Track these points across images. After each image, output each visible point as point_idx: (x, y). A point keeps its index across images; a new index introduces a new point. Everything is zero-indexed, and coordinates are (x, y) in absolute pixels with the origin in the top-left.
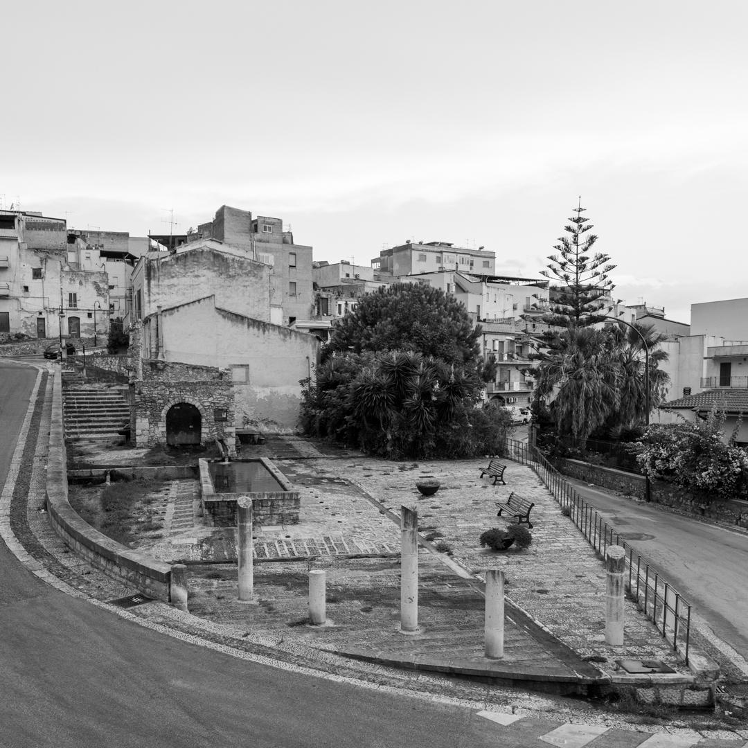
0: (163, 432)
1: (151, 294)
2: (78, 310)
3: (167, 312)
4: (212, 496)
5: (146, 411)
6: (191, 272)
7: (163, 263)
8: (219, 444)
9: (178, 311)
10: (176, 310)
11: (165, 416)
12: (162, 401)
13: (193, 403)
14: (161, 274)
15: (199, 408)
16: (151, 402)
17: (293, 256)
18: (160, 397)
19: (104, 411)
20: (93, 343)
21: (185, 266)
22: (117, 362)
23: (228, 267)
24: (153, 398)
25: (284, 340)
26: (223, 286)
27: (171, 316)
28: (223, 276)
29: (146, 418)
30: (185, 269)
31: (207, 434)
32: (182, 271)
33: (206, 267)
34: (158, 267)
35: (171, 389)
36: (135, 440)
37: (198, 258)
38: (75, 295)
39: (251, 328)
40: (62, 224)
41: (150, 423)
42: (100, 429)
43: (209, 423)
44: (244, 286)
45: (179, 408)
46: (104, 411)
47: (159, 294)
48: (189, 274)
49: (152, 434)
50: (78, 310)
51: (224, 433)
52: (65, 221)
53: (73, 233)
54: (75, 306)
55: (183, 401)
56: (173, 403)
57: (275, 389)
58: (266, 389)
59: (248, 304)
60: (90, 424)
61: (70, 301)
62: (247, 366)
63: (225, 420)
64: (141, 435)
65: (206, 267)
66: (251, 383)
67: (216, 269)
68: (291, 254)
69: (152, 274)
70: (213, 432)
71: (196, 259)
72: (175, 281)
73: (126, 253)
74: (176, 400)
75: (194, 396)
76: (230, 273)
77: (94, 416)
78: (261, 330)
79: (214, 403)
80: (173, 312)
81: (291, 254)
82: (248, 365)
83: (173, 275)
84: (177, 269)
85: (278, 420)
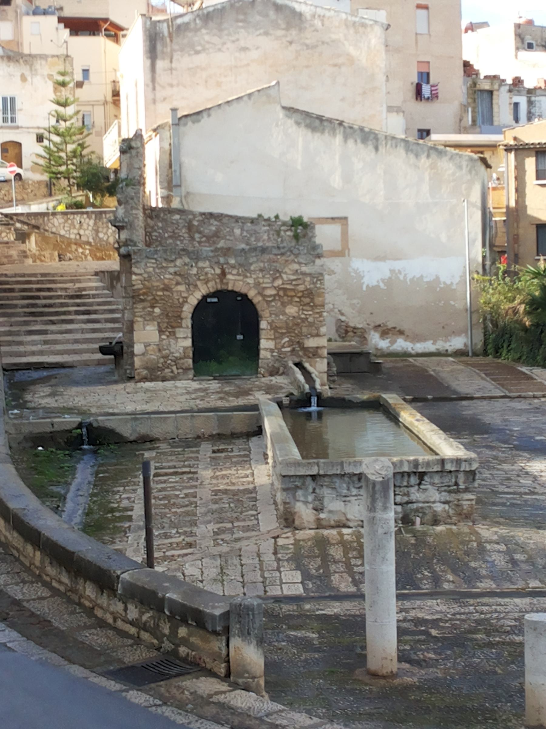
0: (185, 348)
1: (157, 85)
2: (18, 128)
3: (189, 118)
4: (297, 464)
5: (153, 307)
6: (233, 42)
7: (179, 27)
8: (296, 369)
9: (209, 115)
10: (205, 114)
11: (190, 315)
13: (244, 291)
14: (176, 47)
15: (255, 301)
16: (163, 290)
17: (424, 12)
18: (179, 278)
20: (44, 190)
21: (221, 30)
22: (92, 222)
23: (301, 30)
24: (166, 281)
25: (417, 167)
26: (294, 67)
27: (196, 125)
28: (294, 47)
29: (154, 320)
30: (220, 37)
31: (272, 351)
32: (215, 40)
33: (262, 31)
34: (170, 35)
35: (201, 264)
36: (132, 364)
37: (245, 14)
38: (13, 100)
39: (351, 142)
44: (335, 65)
45: (215, 300)
47: (172, 86)
48: (229, 45)
50: (18, 128)
51: (306, 350)
54: (13, 120)
55: (224, 287)
57: (397, 265)
58: (381, 264)
59: (343, 100)
62: (343, 220)
64: (143, 354)
65: (262, 31)
66: (352, 252)
67: (280, 33)
68: (419, 7)
69: (159, 47)
70: (283, 347)
71: (241, 17)
72: (201, 59)
74: (210, 284)
76: (308, 42)
78: (371, 147)
79: (285, 290)
80: (199, 117)
81: (419, 7)
82: (346, 218)
83: (199, 48)
84: (207, 38)
85: (404, 326)
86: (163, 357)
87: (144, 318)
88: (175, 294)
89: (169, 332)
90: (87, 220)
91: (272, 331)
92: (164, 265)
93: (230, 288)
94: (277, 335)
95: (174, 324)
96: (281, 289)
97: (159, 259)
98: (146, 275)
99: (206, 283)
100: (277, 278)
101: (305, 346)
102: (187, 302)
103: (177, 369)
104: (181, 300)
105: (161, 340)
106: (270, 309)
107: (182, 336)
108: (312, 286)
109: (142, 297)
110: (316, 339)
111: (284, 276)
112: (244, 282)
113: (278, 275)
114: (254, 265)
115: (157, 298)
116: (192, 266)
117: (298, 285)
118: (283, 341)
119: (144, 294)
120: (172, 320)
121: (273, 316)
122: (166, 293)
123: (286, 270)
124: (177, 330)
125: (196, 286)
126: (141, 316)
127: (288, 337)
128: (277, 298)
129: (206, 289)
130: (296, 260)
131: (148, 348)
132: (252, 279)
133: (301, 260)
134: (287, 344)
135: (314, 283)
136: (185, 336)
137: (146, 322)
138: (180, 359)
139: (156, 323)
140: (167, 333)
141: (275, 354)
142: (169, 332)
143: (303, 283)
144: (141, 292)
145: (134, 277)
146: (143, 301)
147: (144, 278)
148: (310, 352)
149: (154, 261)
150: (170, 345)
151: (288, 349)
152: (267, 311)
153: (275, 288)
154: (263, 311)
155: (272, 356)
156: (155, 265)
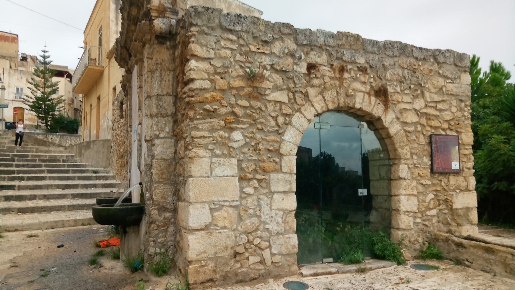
0: (286, 212)
12: (283, 97)
18: (277, 78)
19: (43, 172)
38: (21, 89)
40: (14, 38)
41: (241, 179)
42: (30, 204)
46: (43, 172)
49: (248, 222)
52: (17, 36)
53: (25, 56)
60: (10, 193)
61: (17, 93)
64: (206, 228)
73: (66, 72)
77: (22, 179)
86: (247, 233)
87: (212, 150)
88: (270, 107)
89: (260, 181)
90: (56, 138)
91: (414, 183)
92: (253, 48)
93: (358, 106)
94: (421, 189)
95: (267, 165)
97: (245, 35)
98: (218, 63)
99: (321, 93)
102: (290, 123)
103: (273, 255)
104: (281, 120)
105: (243, 195)
106: (411, 146)
107: (282, 190)
109: (208, 107)
111: (427, 94)
115: (237, 110)
116: (300, 58)
117: (441, 110)
119: (214, 100)
120: (265, 158)
121: (415, 157)
122: (254, 103)
124: (274, 176)
125: (306, 95)
126: (206, 147)
128: (419, 128)
129: (323, 104)
130: (441, 72)
131: (216, 214)
133: (448, 74)
134: (432, 202)
136: (286, 189)
137: (215, 160)
138: (278, 234)
139: (235, 161)
140: (255, 183)
141: (418, 220)
142: (260, 181)
143: (449, 109)
144: (208, 95)
145: (193, 64)
146: (210, 114)
147: (215, 68)
149: (234, 38)
150: (259, 206)
152: (407, 148)
155: (414, 223)
156: (235, 47)
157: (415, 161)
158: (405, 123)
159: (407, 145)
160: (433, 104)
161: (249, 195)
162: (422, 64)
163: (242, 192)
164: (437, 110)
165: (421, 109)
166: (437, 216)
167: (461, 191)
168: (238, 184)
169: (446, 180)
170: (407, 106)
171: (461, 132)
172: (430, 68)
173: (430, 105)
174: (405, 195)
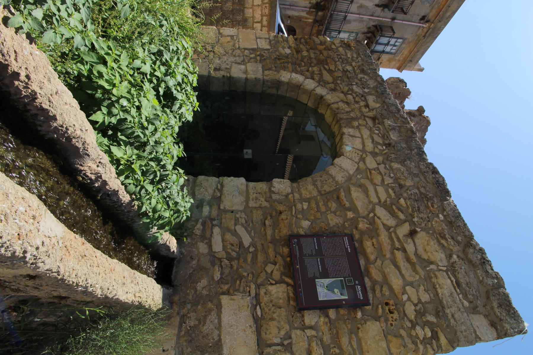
43: (273, 214)
56: (330, 97)
63: (304, 300)
70: (225, 230)
75: (374, 154)
79: (373, 233)
88: (315, 69)
91: (265, 204)
94: (257, 216)
96: (372, 222)
100: (393, 215)
101: (225, 299)
108: (410, 310)
110: (252, 339)
112: (363, 150)
113: (402, 216)
114: (403, 169)
118: (240, 230)
122: (315, 61)
123: (422, 237)
127: (253, 244)
132: (376, 166)
135: (420, 314)
139: (269, 47)
148: (202, 321)
149: (355, 56)
151: (218, 246)
152: (315, 193)
153: (373, 210)
154: (314, 184)
157: (299, 206)
158: (348, 192)
159: (319, 191)
160: (397, 245)
161: (243, 52)
162: (442, 221)
163: (245, 49)
164: (393, 253)
165: (379, 218)
166: (212, 253)
167: (259, 323)
168: (252, 47)
169: (277, 275)
170: (372, 193)
171: (377, 318)
172: (447, 236)
173: (393, 235)
174: (247, 186)
